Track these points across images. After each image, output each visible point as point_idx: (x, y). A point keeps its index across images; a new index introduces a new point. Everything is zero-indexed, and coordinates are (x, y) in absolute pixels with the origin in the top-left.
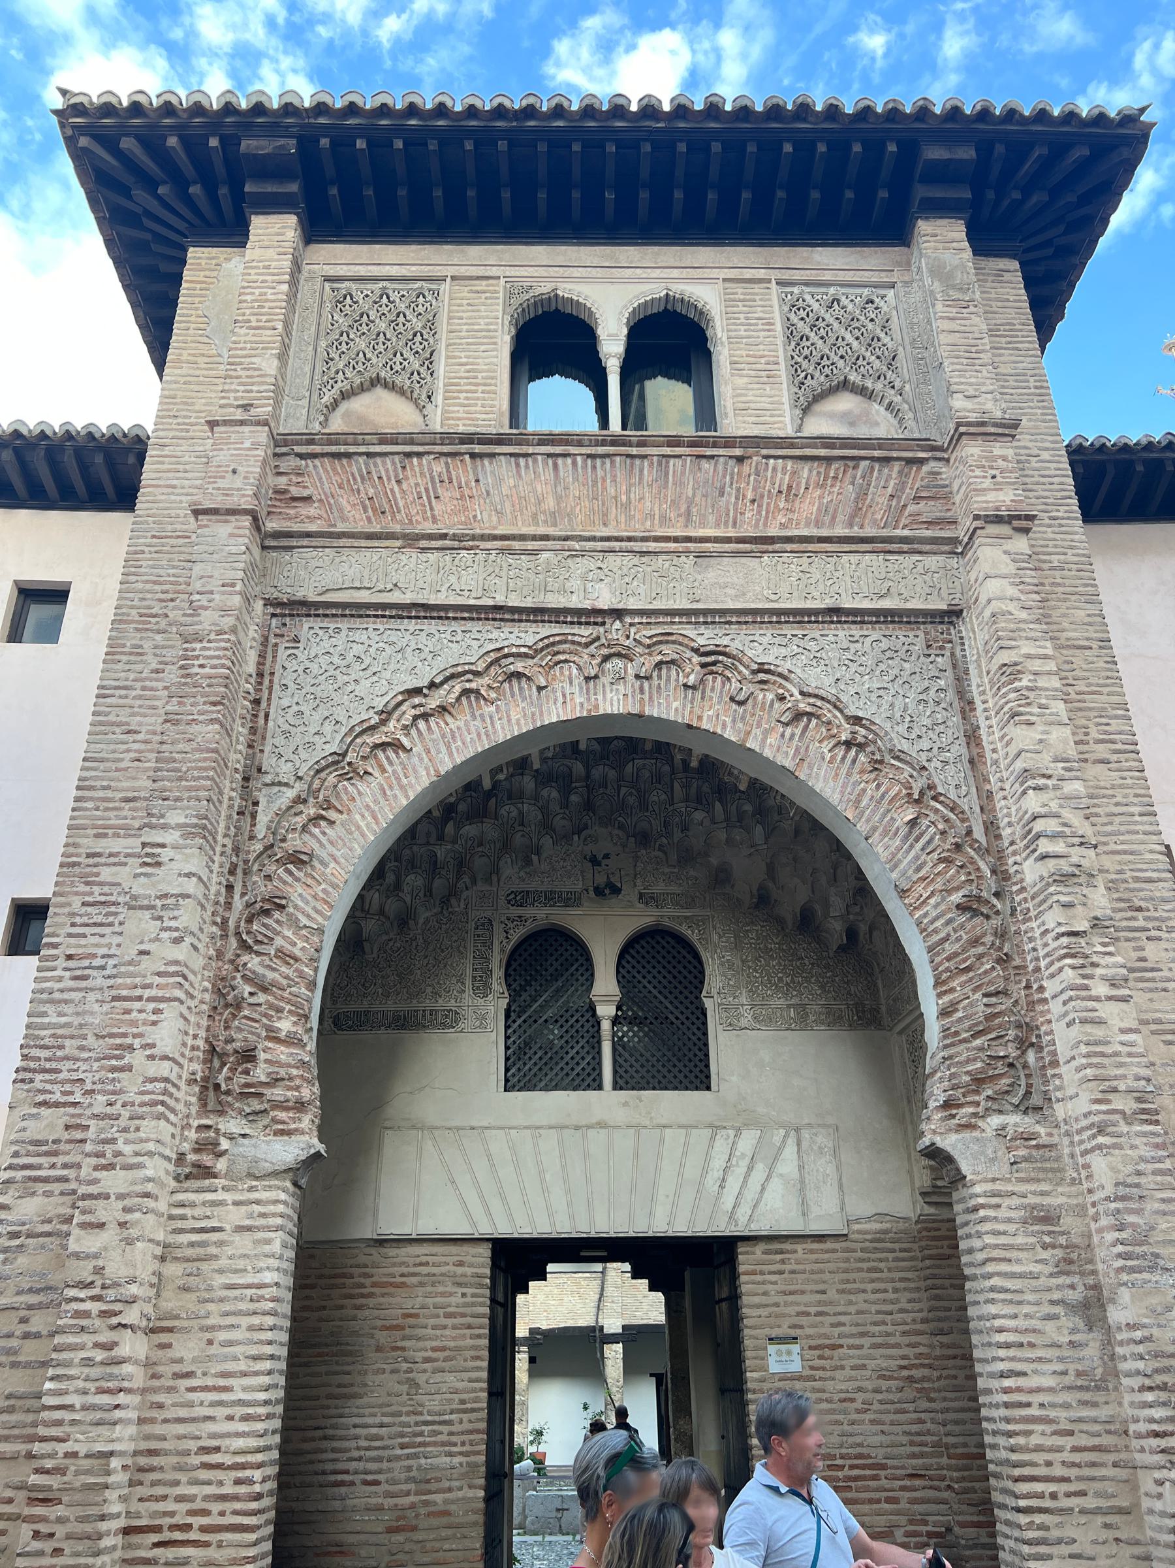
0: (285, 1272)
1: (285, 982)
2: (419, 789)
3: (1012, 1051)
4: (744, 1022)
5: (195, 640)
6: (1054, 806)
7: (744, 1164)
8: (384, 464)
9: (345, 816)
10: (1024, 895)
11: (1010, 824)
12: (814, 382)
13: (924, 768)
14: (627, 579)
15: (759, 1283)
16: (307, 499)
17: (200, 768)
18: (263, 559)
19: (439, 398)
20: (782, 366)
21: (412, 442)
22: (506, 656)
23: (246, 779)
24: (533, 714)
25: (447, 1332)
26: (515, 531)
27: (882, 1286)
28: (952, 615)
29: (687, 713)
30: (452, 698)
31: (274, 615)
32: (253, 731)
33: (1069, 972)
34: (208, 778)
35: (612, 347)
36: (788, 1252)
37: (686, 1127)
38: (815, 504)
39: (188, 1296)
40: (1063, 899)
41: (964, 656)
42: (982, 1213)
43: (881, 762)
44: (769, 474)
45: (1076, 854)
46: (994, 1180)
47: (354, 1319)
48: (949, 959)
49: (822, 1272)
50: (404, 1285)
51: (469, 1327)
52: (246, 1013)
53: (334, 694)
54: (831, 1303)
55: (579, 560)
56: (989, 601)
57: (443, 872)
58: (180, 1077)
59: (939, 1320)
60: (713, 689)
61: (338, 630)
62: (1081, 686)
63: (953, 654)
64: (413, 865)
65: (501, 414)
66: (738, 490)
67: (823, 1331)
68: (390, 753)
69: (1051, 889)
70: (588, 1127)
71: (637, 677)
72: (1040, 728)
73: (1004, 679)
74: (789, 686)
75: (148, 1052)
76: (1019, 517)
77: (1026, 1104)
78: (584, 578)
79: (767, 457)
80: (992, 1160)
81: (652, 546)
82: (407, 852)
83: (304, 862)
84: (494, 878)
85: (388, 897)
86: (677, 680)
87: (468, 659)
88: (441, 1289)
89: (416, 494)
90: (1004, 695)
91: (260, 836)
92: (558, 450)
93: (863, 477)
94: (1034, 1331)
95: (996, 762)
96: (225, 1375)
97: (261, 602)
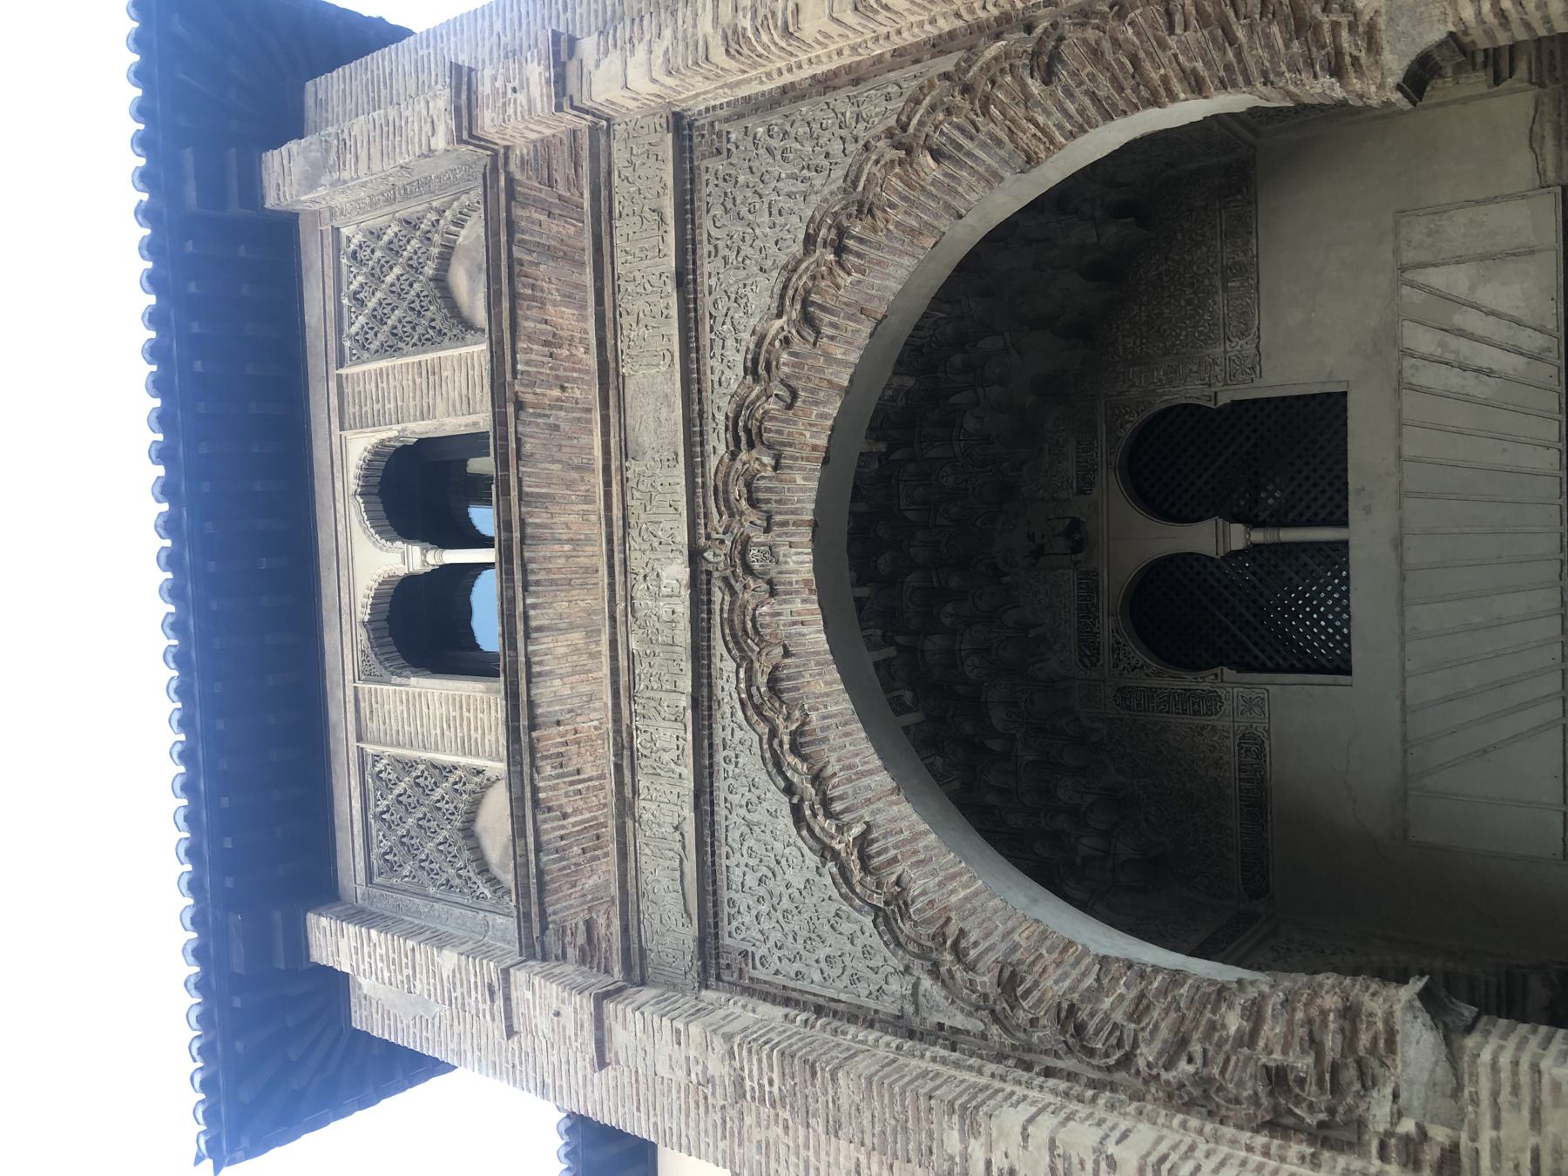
1: (1173, 1015)
2: (915, 816)
4: (1250, 349)
5: (742, 1086)
7: (1454, 342)
8: (547, 832)
9: (952, 915)
12: (438, 318)
13: (866, 147)
14: (656, 544)
16: (589, 925)
17: (892, 1102)
18: (655, 985)
20: (422, 357)
21: (521, 799)
22: (750, 696)
23: (911, 1035)
24: (818, 664)
26: (607, 682)
28: (680, 125)
29: (809, 465)
31: (718, 978)
32: (852, 1019)
34: (903, 1093)
35: (415, 558)
37: (1400, 424)
43: (861, 204)
48: (1120, 89)
52: (1216, 1071)
56: (654, 81)
60: (780, 432)
61: (731, 903)
63: (727, 120)
65: (489, 691)
66: (552, 407)
73: (746, 51)
74: (772, 332)
76: (556, 54)
78: (656, 597)
79: (515, 372)
81: (617, 513)
83: (1013, 974)
86: (770, 479)
87: (756, 744)
89: (579, 801)
90: (765, 47)
91: (982, 1027)
92: (520, 627)
93: (530, 252)
95: (854, 49)
97: (704, 992)
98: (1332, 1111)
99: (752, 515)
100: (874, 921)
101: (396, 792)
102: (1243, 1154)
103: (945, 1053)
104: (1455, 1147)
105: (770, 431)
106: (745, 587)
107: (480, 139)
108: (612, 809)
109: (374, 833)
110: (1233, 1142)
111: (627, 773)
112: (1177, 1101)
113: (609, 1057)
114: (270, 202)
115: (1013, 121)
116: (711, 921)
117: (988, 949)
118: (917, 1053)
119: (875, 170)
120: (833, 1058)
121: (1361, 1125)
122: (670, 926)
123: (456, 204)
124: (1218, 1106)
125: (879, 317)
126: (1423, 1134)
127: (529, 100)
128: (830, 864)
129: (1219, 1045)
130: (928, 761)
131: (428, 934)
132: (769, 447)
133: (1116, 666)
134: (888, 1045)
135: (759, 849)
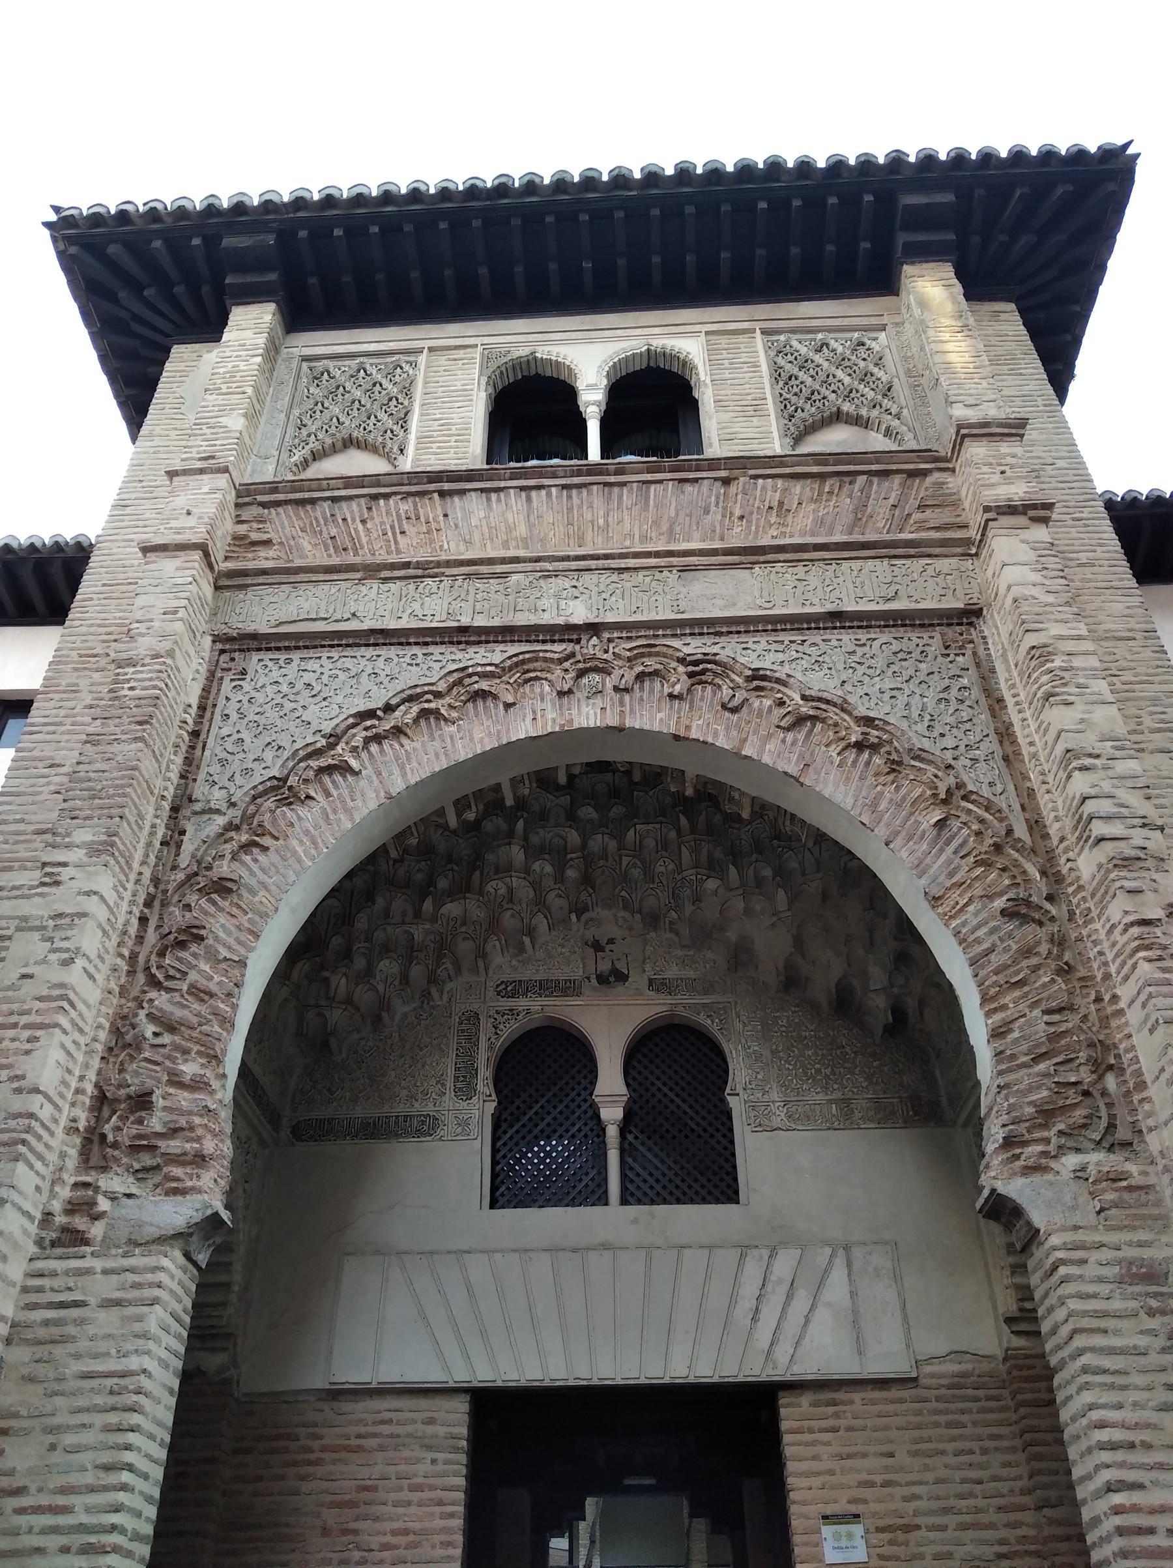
0: (164, 1364)
3: (1085, 1075)
4: (776, 1122)
5: (128, 665)
6: (1106, 786)
7: (782, 1291)
9: (281, 842)
10: (1083, 894)
11: (1057, 819)
12: (805, 415)
13: (949, 767)
15: (807, 1444)
16: (268, 543)
19: (411, 450)
20: (770, 400)
21: (379, 485)
22: (470, 676)
23: (175, 809)
24: (499, 732)
25: (413, 1510)
27: (967, 1445)
28: (970, 615)
29: (673, 723)
30: (408, 719)
31: (222, 652)
32: (188, 761)
33: (1145, 967)
34: (125, 795)
35: (592, 399)
36: (843, 1403)
37: (711, 1247)
38: (809, 516)
39: (32, 1388)
40: (1128, 884)
41: (989, 655)
42: (1062, 1270)
43: (900, 763)
44: (758, 493)
45: (1138, 837)
46: (1076, 1228)
47: (297, 1493)
49: (887, 1428)
50: (359, 1449)
51: (440, 1503)
52: (147, 1054)
53: (279, 722)
54: (900, 1469)
55: (553, 580)
56: (1009, 587)
57: (422, 956)
58: (56, 1121)
59: (1044, 1487)
60: (702, 699)
61: (289, 661)
62: (1128, 676)
63: (975, 654)
64: (386, 949)
66: (725, 508)
67: (892, 1506)
68: (338, 778)
69: (1112, 876)
70: (588, 1249)
71: (616, 689)
72: (1082, 707)
75: (15, 1085)
76: (1034, 507)
77: (1110, 1139)
78: (557, 596)
80: (1073, 1208)
81: (631, 563)
82: (380, 935)
83: (230, 891)
84: (481, 964)
85: (357, 985)
86: (662, 691)
87: (428, 680)
88: (406, 1453)
89: (378, 532)
91: (183, 866)
92: (531, 482)
94: (1148, 1426)
95: (1034, 756)
96: (66, 1490)
97: (210, 639)
98: (115, 1145)
99: (630, 676)
100: (274, 777)
101: (384, 382)
102: (77, 1073)
103: (159, 835)
104: (86, 1242)
105: (703, 691)
106: (566, 670)
107: (961, 444)
108: (369, 559)
109: (346, 363)
110: (87, 1066)
111: (402, 573)
112: (120, 1023)
113: (152, 556)
114: (907, 269)
115: (970, 886)
116: (273, 645)
117: (248, 870)
118: (159, 812)
119: (929, 774)
120: (154, 740)
121: (104, 1169)
122: (263, 611)
123: (905, 428)
124: (117, 1056)
125: (801, 780)
126: (96, 1217)
127: (993, 485)
128: (324, 742)
129: (169, 1057)
130: (414, 830)
131: (257, 407)
132: (689, 690)
133: (498, 1012)
134: (166, 789)
135: (336, 684)
